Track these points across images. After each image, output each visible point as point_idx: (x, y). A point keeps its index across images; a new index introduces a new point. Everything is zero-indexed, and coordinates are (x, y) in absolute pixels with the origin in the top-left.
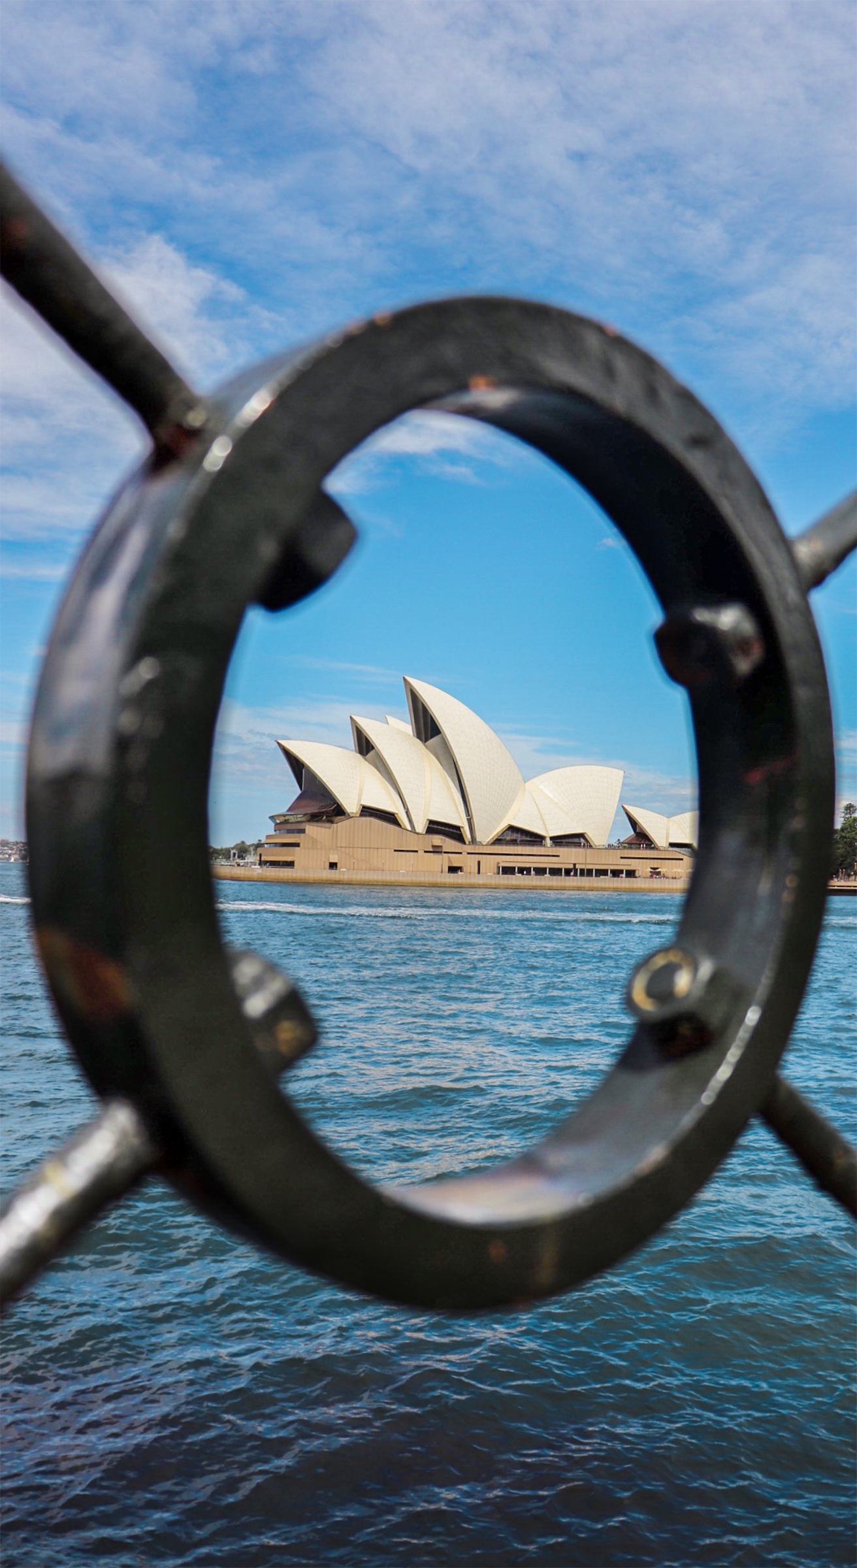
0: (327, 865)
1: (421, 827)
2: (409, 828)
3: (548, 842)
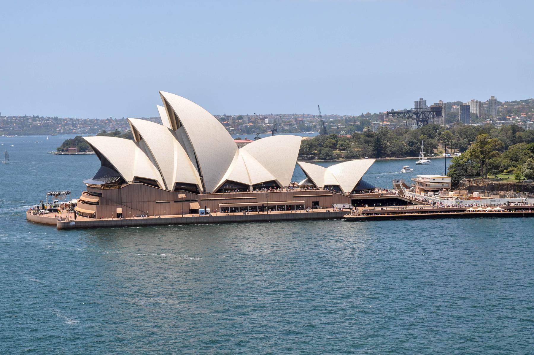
1: (171, 188)
2: (164, 189)
3: (251, 188)
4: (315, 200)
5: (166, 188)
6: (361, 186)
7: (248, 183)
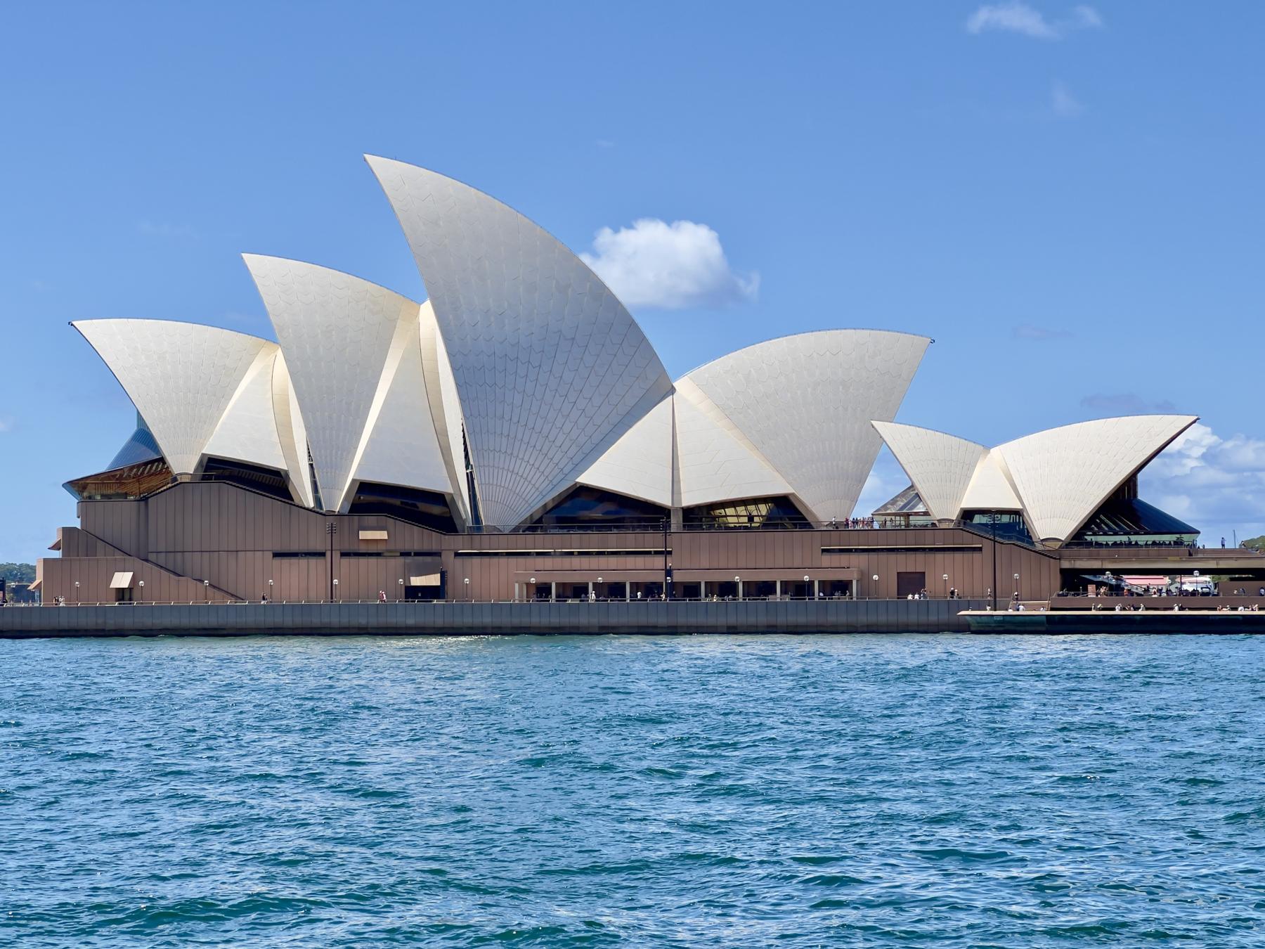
0: (113, 595)
1: (338, 500)
2: (311, 503)
3: (676, 521)
5: (318, 500)
7: (662, 498)
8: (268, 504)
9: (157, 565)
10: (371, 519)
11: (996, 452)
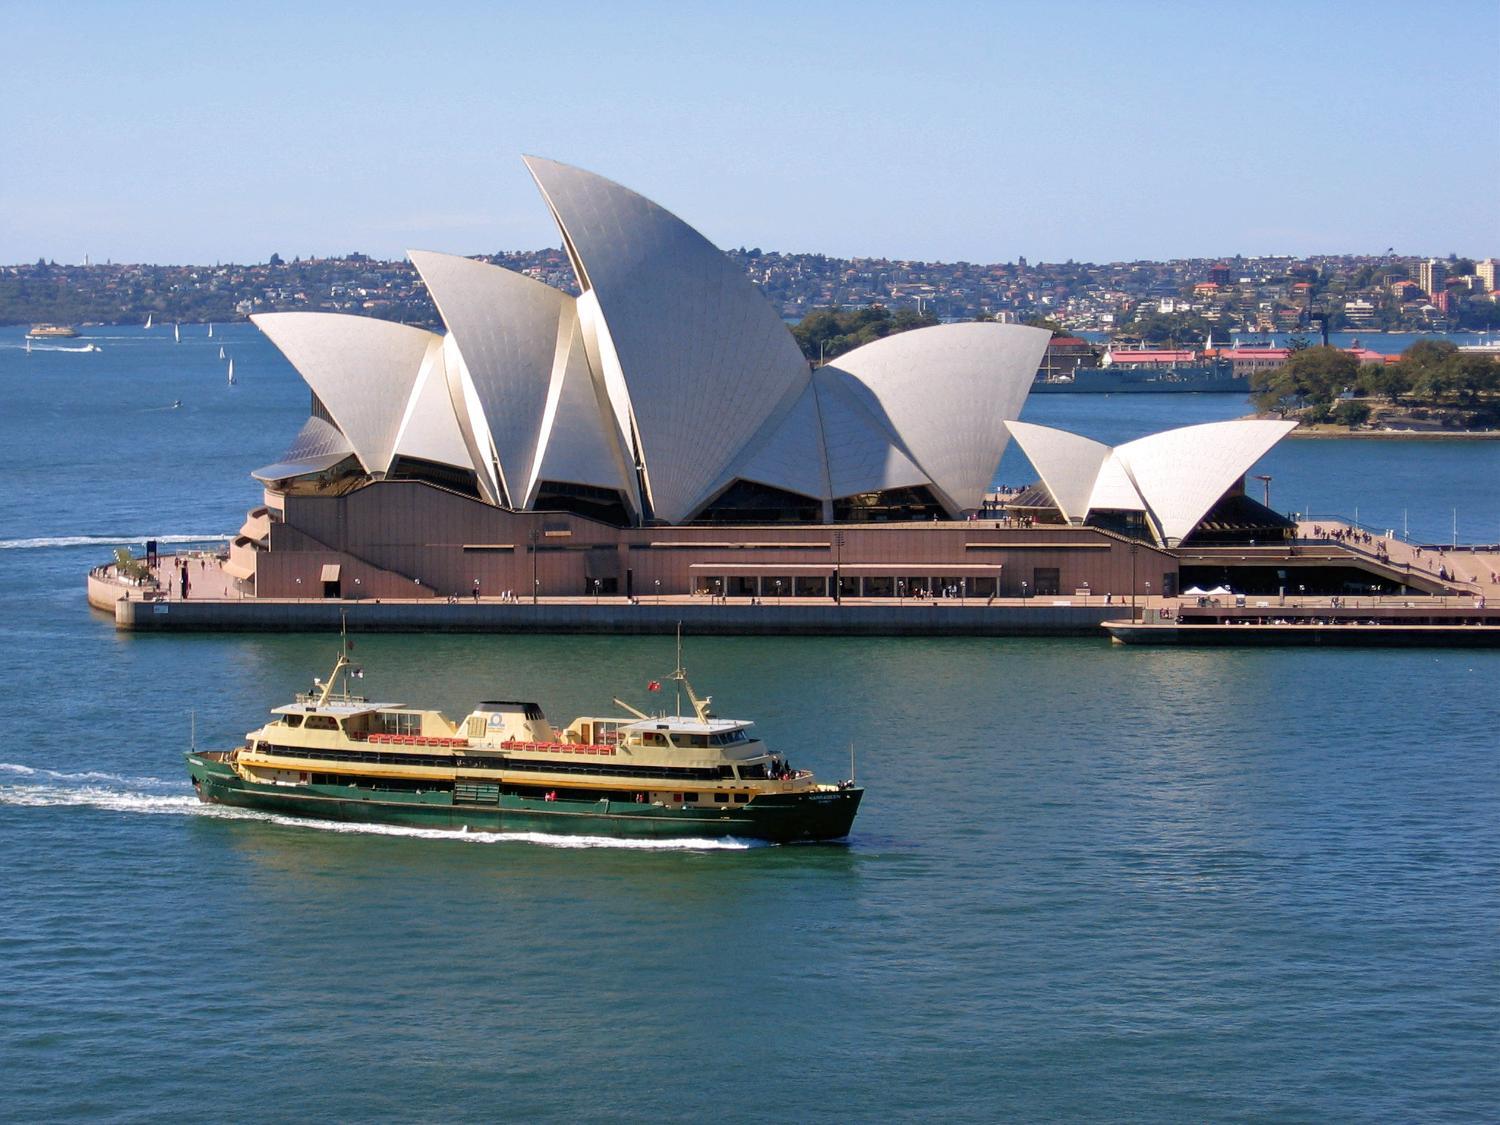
0: (322, 587)
3: (827, 512)
4: (1043, 561)
6: (1237, 514)
8: (460, 501)
9: (356, 556)
10: (555, 516)
11: (1121, 451)
